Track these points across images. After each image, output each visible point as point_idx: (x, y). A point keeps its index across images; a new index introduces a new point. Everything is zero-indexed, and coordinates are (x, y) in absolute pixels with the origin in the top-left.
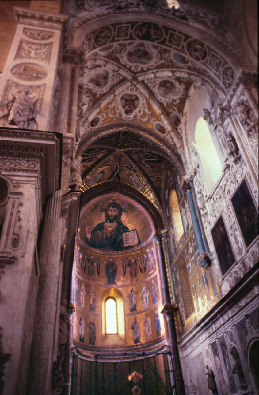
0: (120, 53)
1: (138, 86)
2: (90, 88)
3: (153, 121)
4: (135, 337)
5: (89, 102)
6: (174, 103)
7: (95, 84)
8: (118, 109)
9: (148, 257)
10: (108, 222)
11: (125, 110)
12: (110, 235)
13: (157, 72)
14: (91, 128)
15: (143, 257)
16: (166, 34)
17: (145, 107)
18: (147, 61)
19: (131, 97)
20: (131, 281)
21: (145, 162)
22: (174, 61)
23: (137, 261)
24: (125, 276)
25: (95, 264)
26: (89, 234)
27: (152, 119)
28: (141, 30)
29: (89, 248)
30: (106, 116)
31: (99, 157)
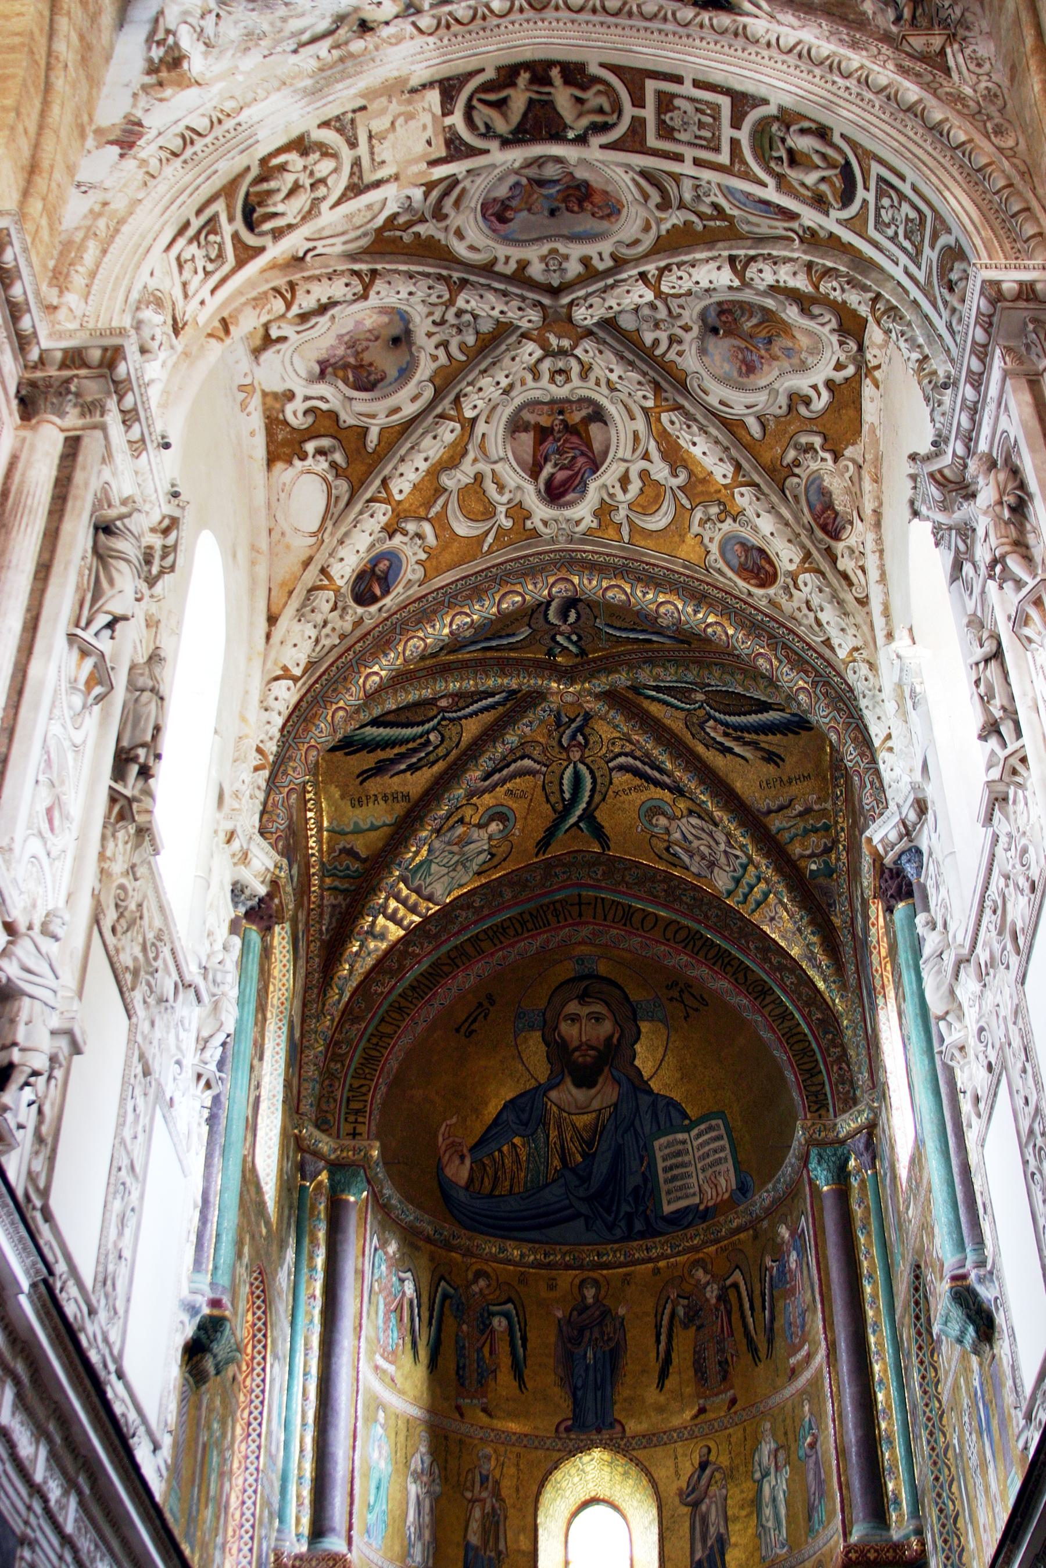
0: (438, 214)
1: (586, 350)
2: (324, 406)
3: (702, 523)
5: (330, 478)
6: (803, 410)
7: (346, 381)
8: (501, 488)
9: (783, 1270)
10: (568, 1081)
11: (542, 487)
12: (584, 1155)
13: (662, 271)
14: (360, 610)
15: (763, 1269)
16: (639, 102)
17: (646, 456)
18: (605, 225)
19: (561, 413)
20: (702, 1410)
21: (726, 735)
22: (729, 210)
23: (732, 1296)
24: (671, 1383)
25: (499, 1324)
26: (462, 1158)
27: (698, 514)
28: (500, 105)
29: (463, 1238)
30: (437, 537)
31: (466, 738)
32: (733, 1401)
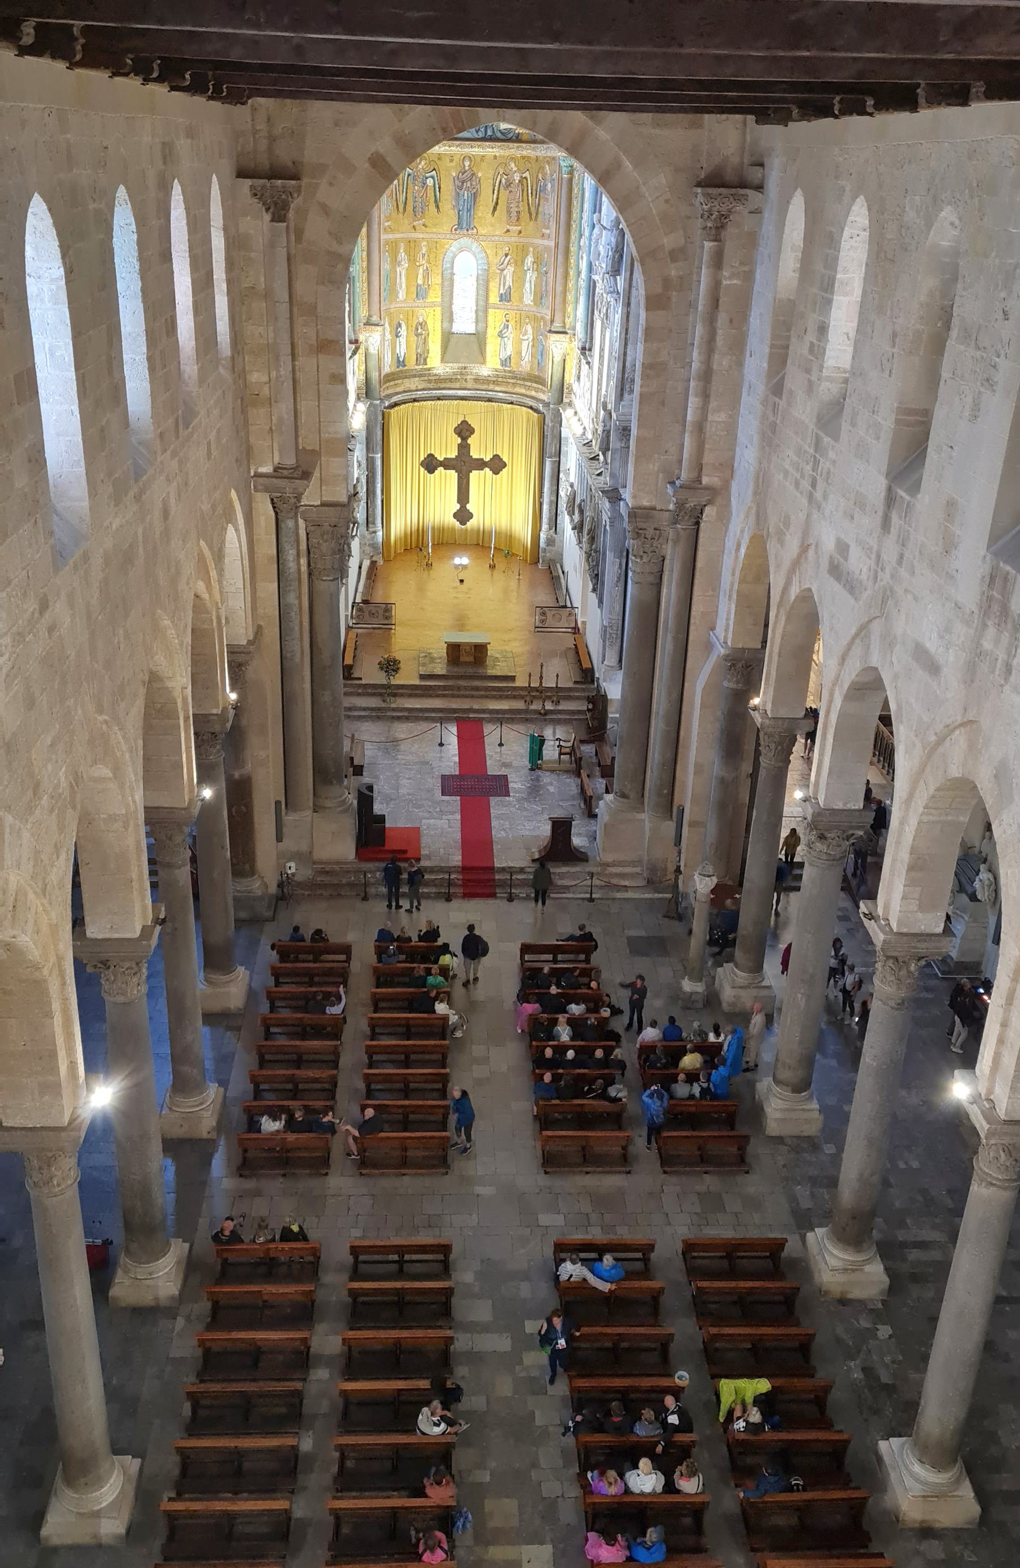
4: (503, 356)
20: (508, 231)
25: (430, 182)
32: (520, 232)
